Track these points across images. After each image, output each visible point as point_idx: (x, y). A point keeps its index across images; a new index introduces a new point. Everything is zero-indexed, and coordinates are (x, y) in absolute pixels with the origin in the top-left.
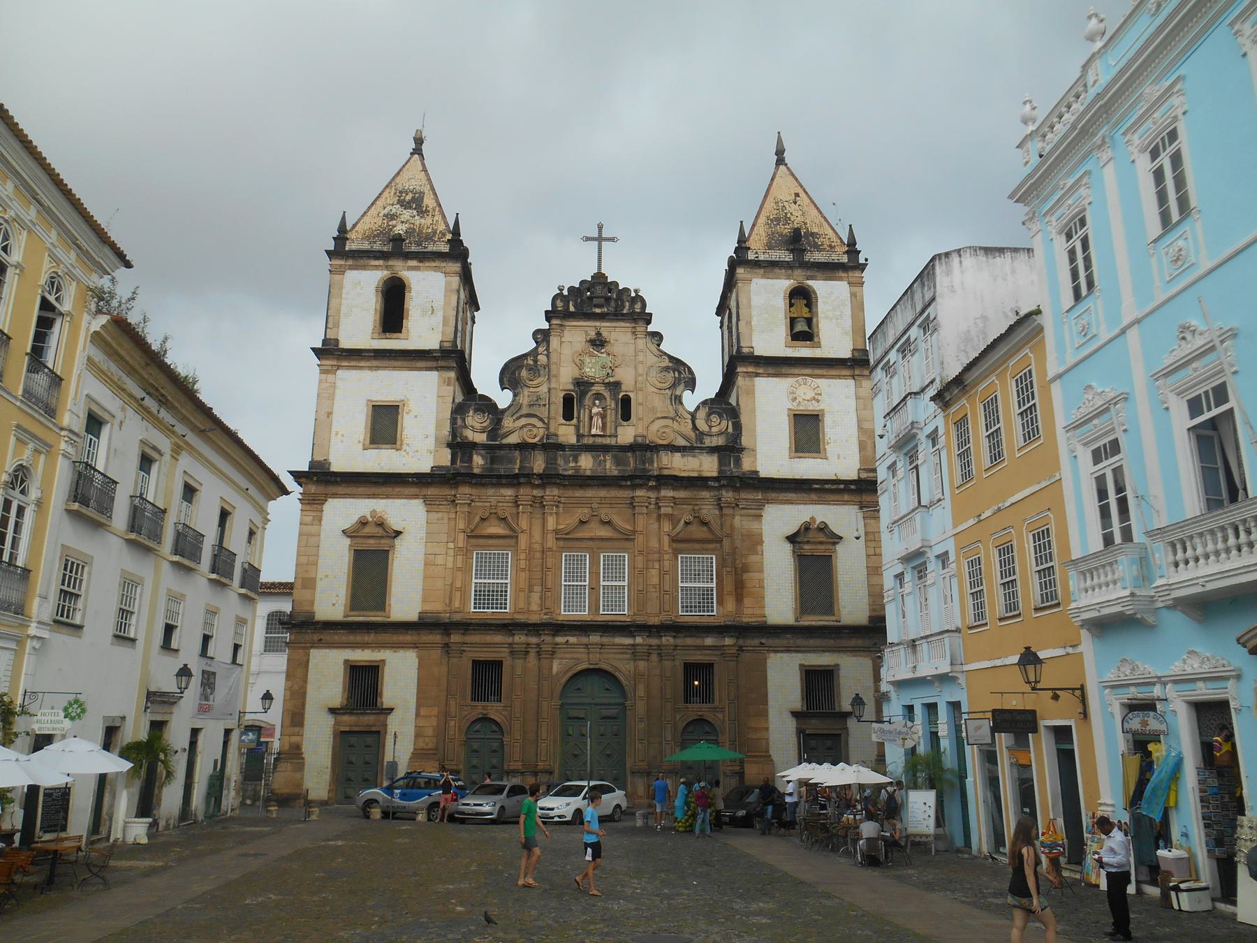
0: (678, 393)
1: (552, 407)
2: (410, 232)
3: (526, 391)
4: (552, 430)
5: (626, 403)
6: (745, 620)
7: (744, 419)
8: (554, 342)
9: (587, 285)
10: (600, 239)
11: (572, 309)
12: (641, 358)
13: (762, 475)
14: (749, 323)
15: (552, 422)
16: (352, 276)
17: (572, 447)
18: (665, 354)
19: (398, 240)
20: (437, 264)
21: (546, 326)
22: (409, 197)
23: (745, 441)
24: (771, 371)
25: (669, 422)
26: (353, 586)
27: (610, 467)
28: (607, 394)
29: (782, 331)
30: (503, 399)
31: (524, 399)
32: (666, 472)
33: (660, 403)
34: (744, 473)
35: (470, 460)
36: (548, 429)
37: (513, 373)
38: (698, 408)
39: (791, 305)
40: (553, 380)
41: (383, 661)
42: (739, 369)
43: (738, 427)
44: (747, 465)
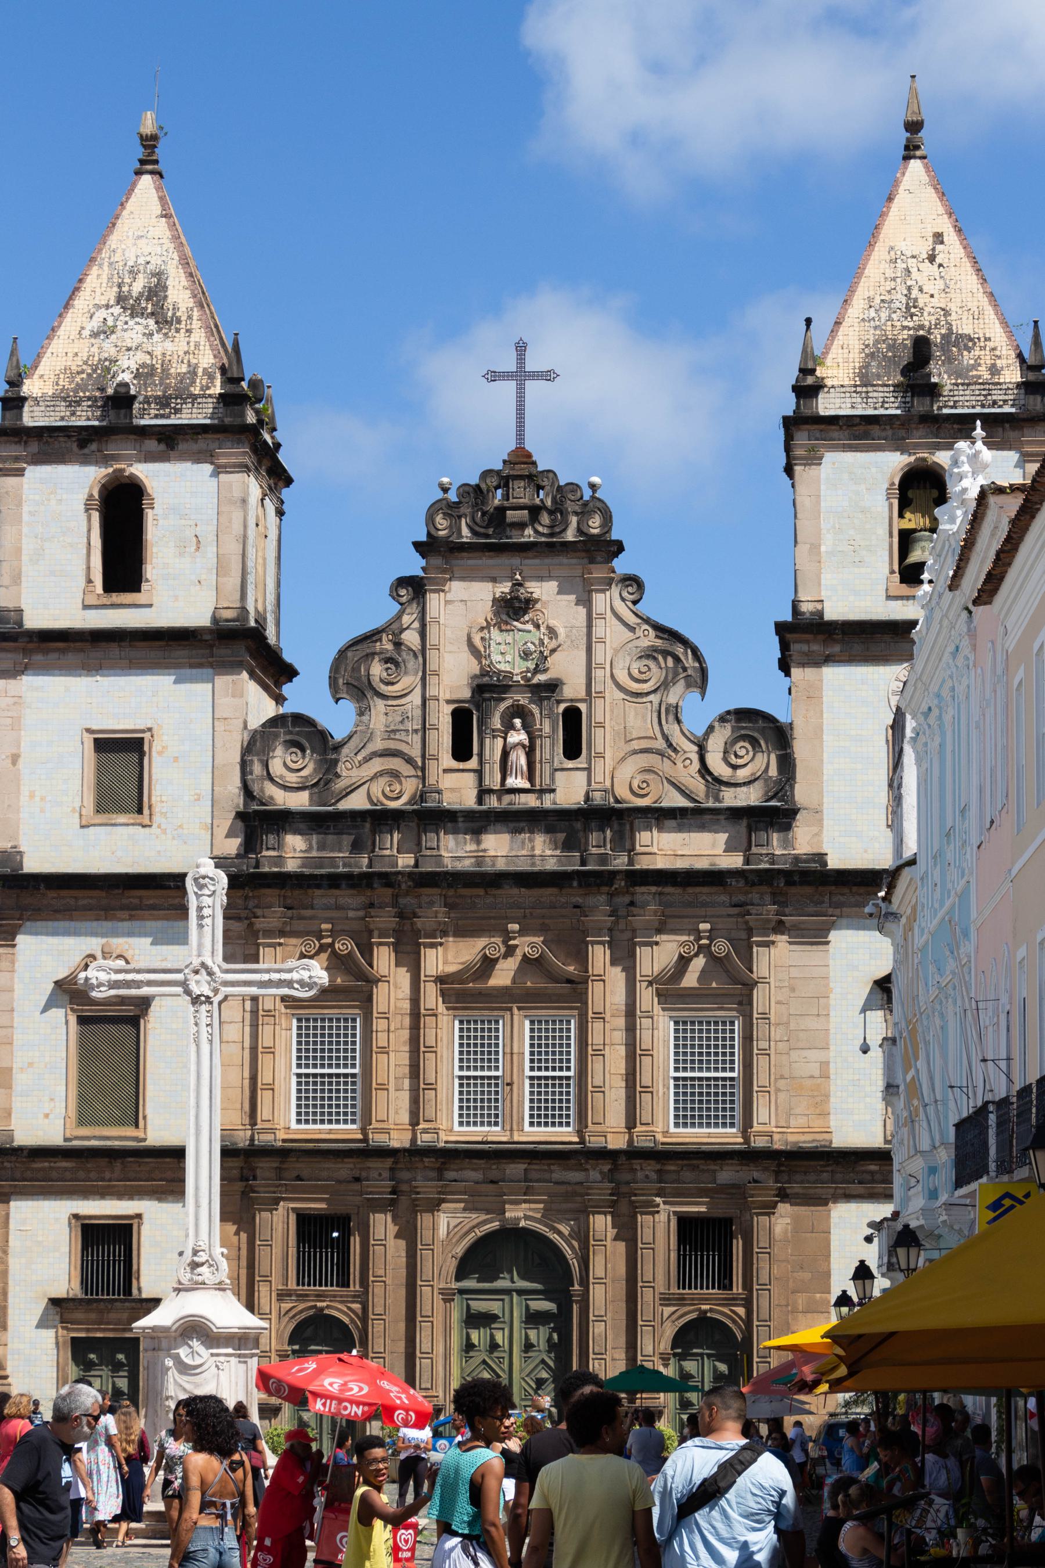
0: (672, 699)
1: (432, 735)
2: (145, 373)
3: (379, 705)
4: (431, 780)
5: (572, 719)
6: (792, 1138)
7: (800, 749)
8: (433, 601)
9: (493, 481)
10: (521, 376)
11: (465, 531)
12: (599, 629)
13: (834, 862)
14: (815, 548)
15: (432, 766)
16: (37, 475)
17: (469, 815)
18: (647, 621)
19: (121, 401)
20: (202, 444)
21: (414, 565)
22: (138, 287)
23: (801, 793)
24: (857, 648)
25: (654, 760)
26: (81, 1083)
27: (541, 852)
28: (535, 709)
29: (881, 562)
30: (338, 719)
31: (379, 715)
32: (643, 864)
33: (640, 720)
34: (797, 859)
35: (280, 846)
36: (424, 778)
37: (356, 669)
38: (711, 729)
39: (904, 504)
40: (432, 680)
41: (139, 1216)
42: (795, 648)
43: (787, 764)
44: (803, 840)
